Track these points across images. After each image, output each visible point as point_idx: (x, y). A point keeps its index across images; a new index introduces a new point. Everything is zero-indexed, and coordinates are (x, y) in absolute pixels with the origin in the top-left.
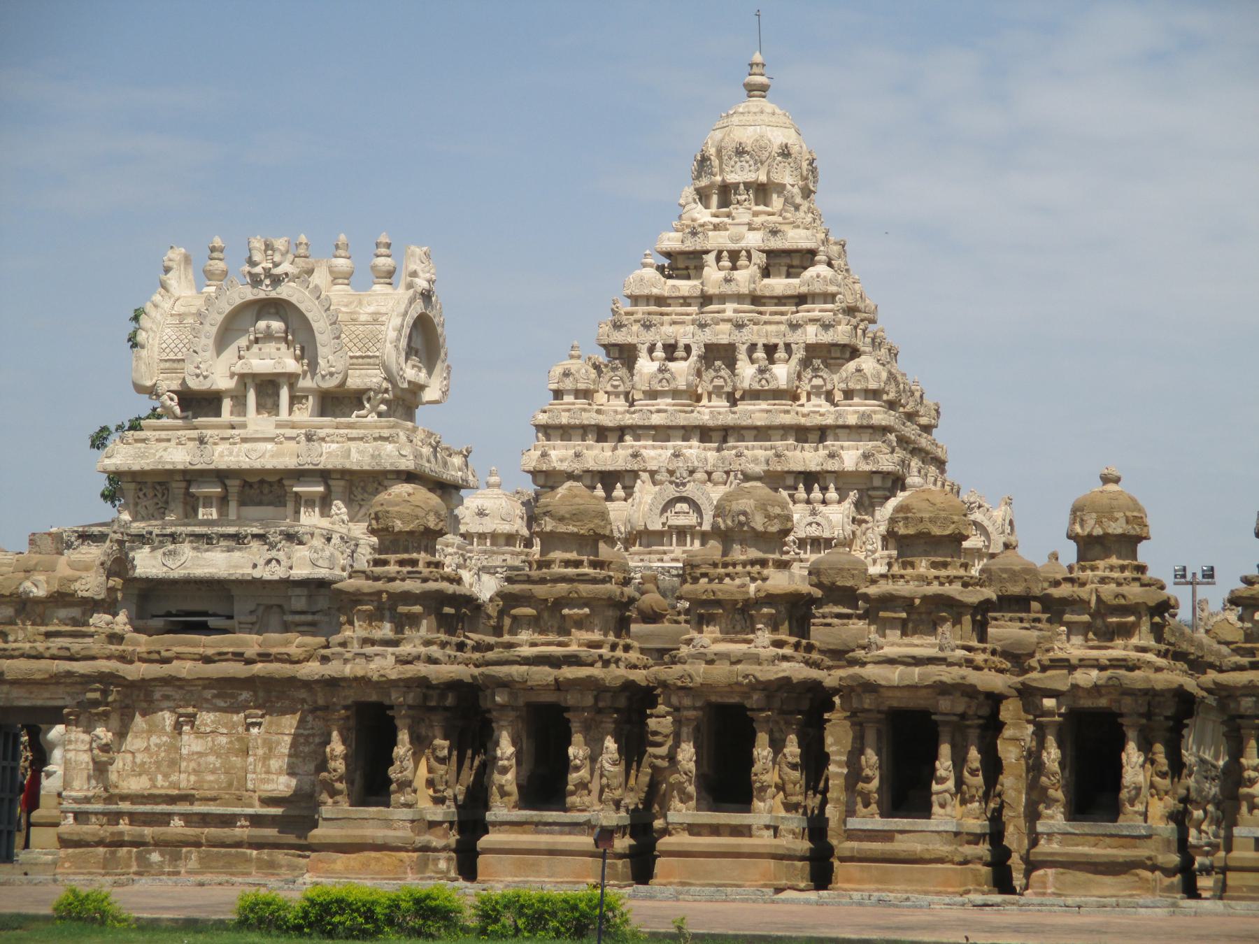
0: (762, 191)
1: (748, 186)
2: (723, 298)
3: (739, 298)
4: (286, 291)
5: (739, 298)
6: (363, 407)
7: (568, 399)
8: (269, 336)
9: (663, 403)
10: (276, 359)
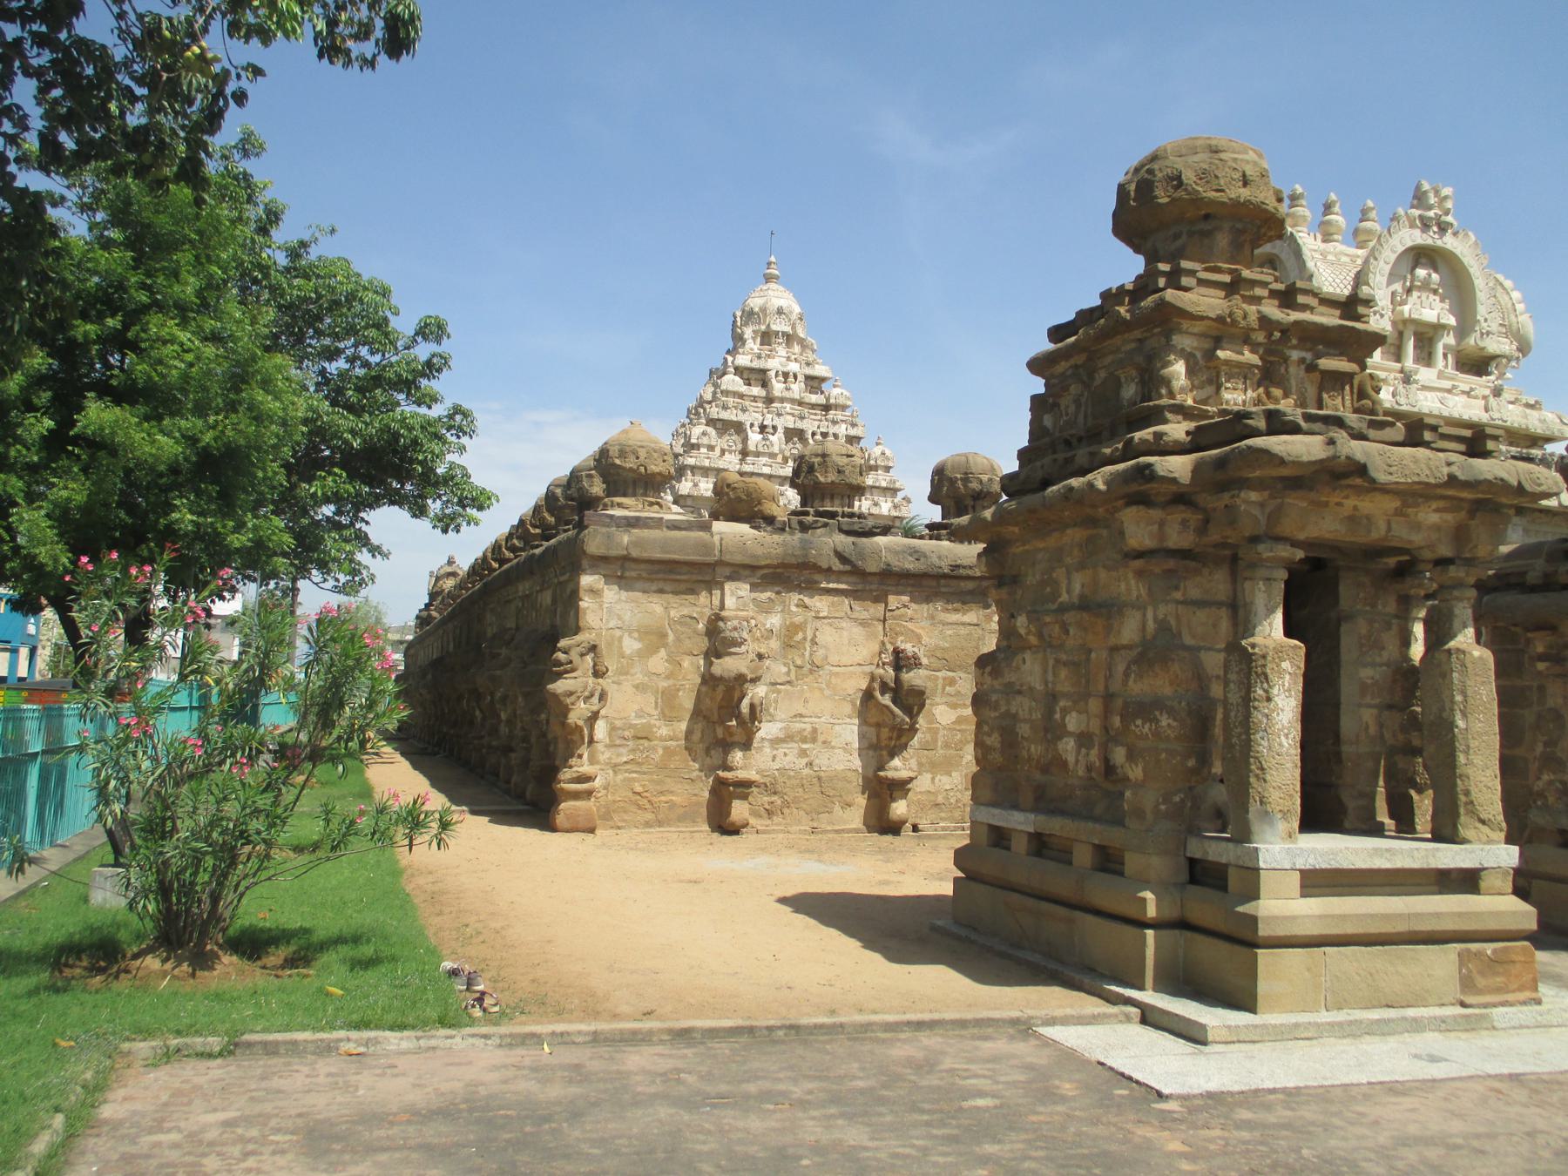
0: (789, 338)
1: (784, 333)
2: (782, 400)
3: (792, 401)
4: (1449, 242)
5: (792, 401)
6: (1488, 374)
7: (703, 450)
8: (1426, 286)
9: (764, 460)
10: (1431, 310)
